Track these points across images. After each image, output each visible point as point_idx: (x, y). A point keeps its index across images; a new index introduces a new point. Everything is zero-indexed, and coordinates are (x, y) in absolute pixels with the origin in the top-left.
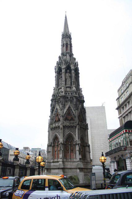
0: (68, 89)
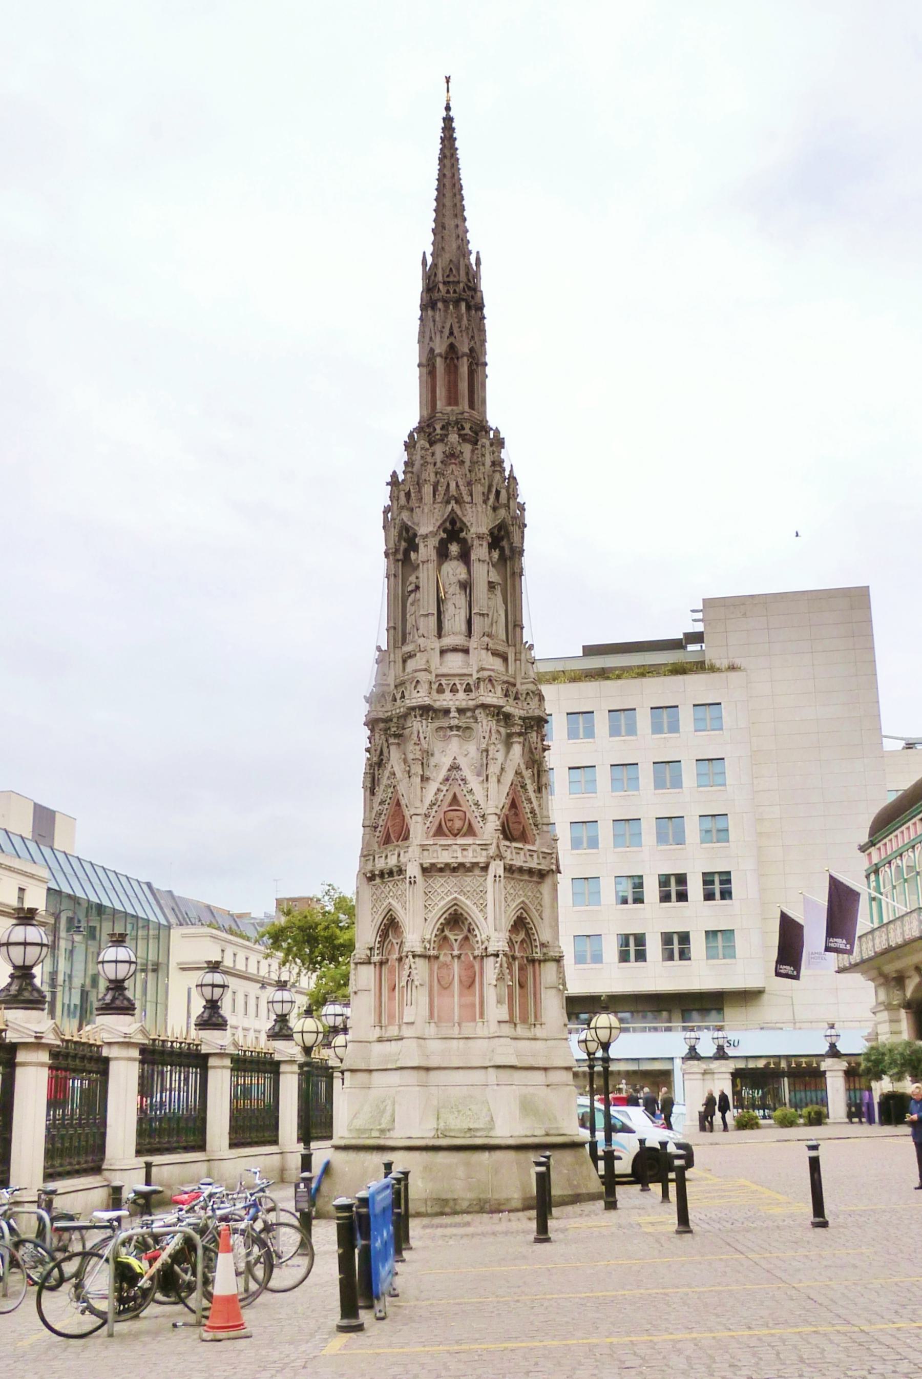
0: (454, 663)
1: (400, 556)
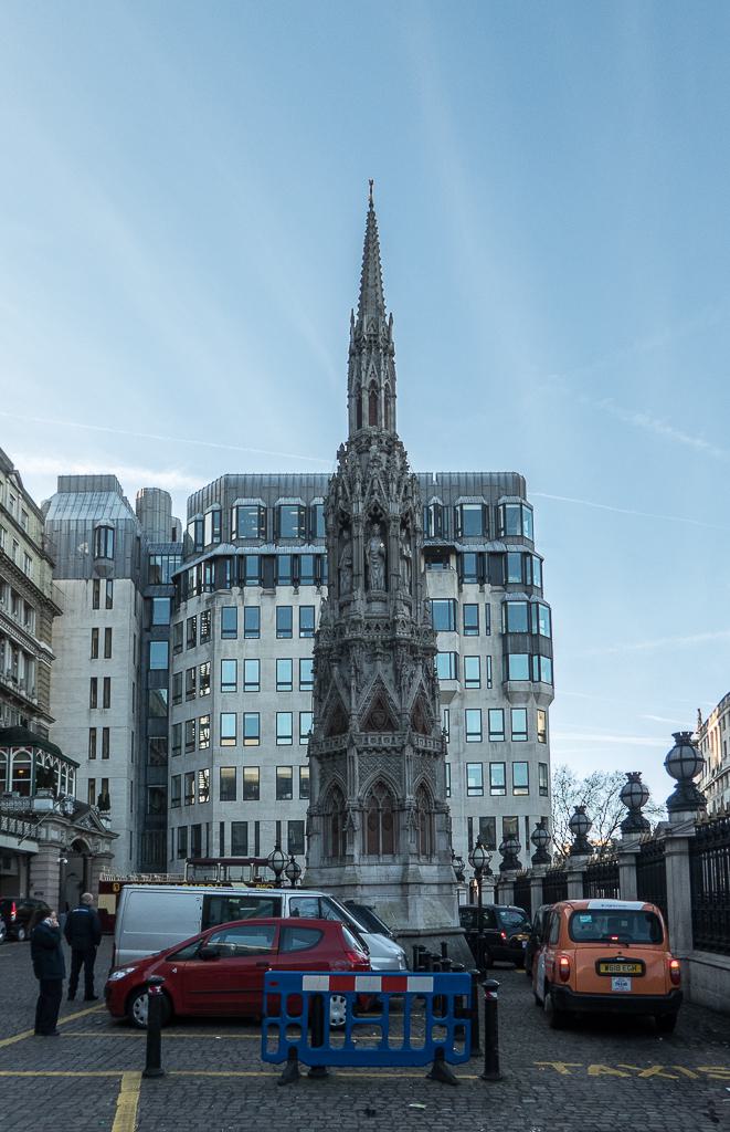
1: (337, 534)
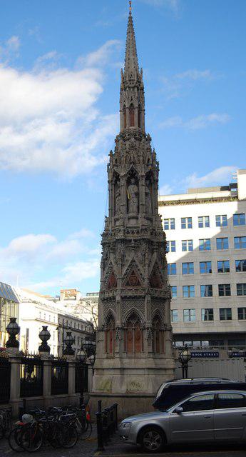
0: (133, 223)
